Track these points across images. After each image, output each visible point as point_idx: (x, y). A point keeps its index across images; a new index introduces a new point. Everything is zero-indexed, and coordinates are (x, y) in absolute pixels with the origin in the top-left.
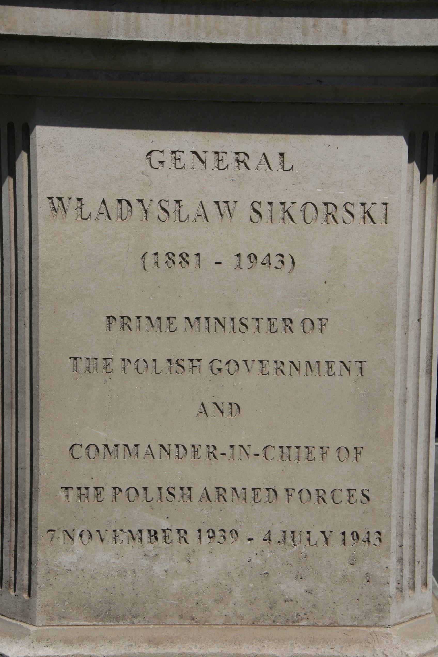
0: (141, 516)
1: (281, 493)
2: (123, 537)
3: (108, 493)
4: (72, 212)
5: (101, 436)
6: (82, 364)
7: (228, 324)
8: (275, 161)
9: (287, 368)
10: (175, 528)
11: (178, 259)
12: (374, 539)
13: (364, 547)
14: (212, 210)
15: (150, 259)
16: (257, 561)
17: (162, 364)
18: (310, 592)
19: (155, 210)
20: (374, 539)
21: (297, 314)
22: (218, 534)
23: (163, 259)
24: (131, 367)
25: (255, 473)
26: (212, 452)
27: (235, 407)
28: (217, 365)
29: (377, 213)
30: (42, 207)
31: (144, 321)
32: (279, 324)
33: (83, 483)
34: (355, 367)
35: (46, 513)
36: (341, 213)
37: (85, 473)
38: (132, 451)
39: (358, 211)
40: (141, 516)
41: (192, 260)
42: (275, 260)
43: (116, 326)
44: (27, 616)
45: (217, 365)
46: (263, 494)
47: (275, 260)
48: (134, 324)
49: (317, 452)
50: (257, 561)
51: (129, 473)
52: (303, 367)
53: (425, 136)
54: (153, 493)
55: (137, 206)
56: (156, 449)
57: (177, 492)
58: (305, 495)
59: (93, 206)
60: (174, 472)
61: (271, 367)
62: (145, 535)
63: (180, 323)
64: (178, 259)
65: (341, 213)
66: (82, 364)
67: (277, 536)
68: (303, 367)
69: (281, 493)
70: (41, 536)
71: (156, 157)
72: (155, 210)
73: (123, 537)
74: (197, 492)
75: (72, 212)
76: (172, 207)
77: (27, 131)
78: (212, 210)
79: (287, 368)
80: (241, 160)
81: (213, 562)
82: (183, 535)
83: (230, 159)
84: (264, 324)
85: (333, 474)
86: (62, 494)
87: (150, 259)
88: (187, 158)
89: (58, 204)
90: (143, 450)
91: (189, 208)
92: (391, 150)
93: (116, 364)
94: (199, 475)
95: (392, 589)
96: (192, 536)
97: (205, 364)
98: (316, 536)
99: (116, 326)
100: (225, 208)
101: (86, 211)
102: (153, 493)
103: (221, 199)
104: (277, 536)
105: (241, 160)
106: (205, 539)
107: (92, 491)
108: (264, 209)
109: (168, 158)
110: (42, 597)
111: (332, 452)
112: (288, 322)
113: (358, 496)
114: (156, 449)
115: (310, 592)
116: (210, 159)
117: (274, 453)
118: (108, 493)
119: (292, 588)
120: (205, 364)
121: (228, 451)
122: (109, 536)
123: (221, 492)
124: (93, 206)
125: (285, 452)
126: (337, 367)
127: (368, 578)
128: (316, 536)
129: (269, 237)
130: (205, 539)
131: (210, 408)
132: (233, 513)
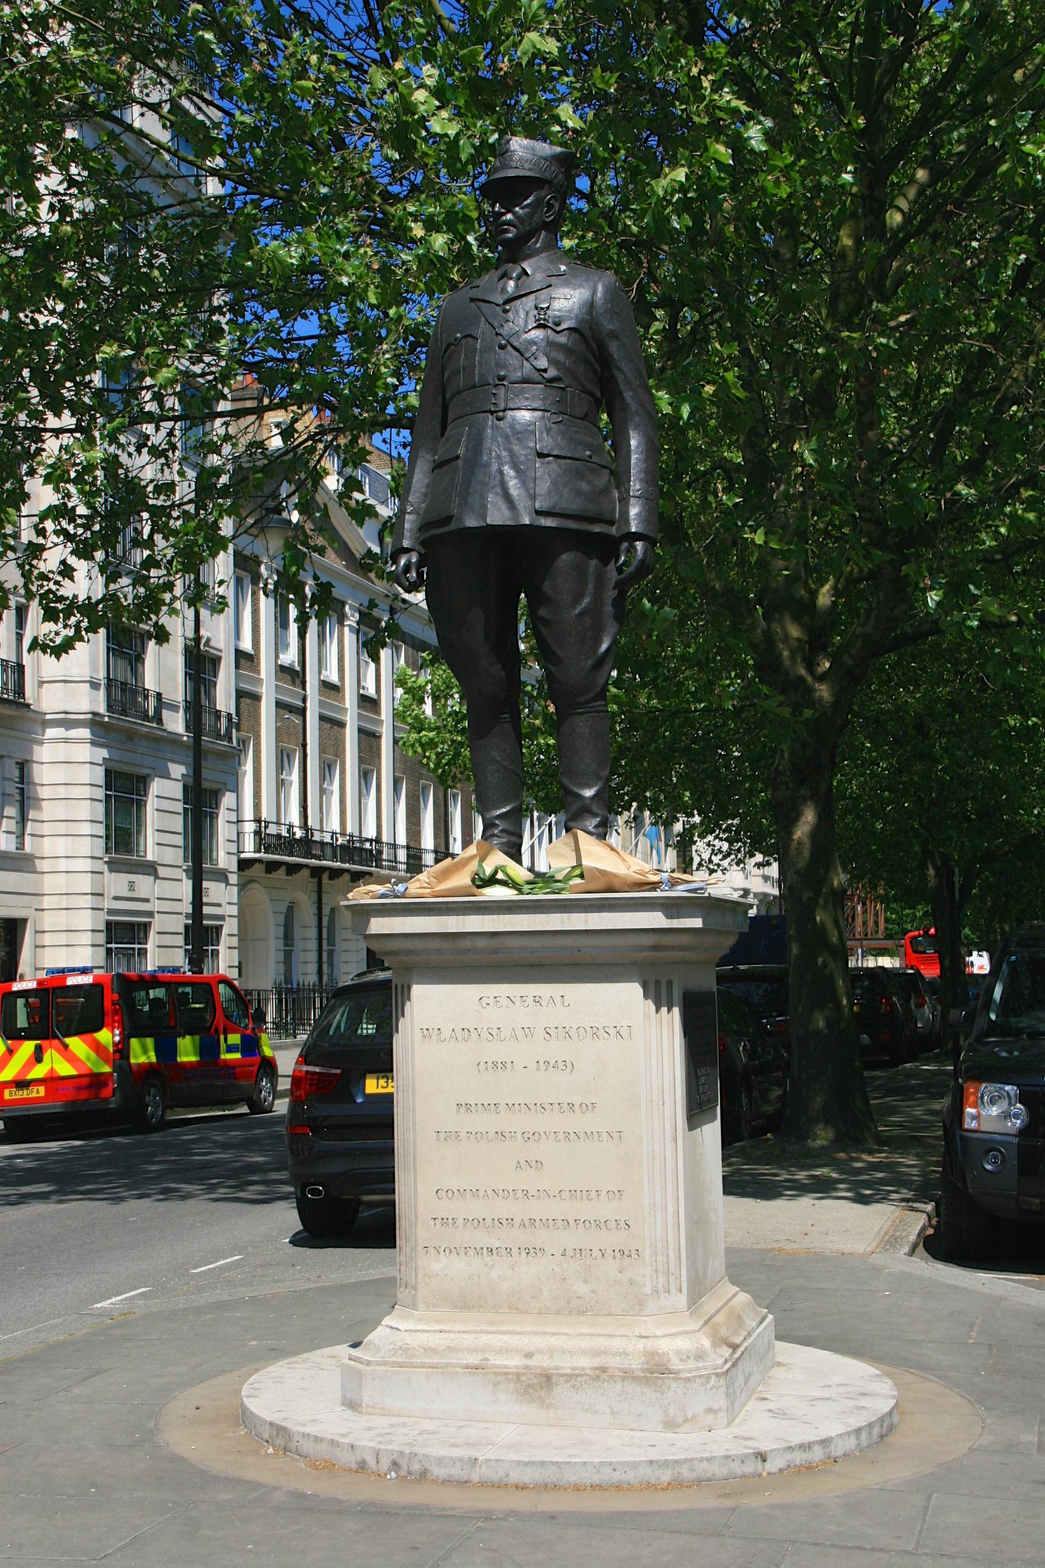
0: (482, 1238)
3: (460, 1222)
4: (434, 1037)
5: (454, 1184)
6: (442, 1136)
7: (533, 1107)
8: (558, 1000)
9: (572, 1137)
12: (634, 1255)
13: (628, 1260)
14: (520, 1033)
15: (482, 1065)
16: (557, 1270)
17: (492, 1135)
18: (593, 1291)
20: (634, 1255)
23: (490, 1065)
24: (473, 1137)
25: (554, 1209)
28: (527, 1135)
29: (625, 1032)
32: (565, 1107)
34: (616, 1136)
36: (602, 1033)
37: (445, 1208)
38: (475, 1193)
39: (612, 1031)
40: (482, 1238)
41: (509, 1065)
42: (561, 1065)
45: (527, 1135)
46: (560, 1223)
47: (561, 1065)
48: (473, 1108)
49: (593, 1194)
50: (557, 1270)
51: (474, 1209)
52: (582, 1135)
53: (658, 983)
54: (489, 1222)
56: (490, 1192)
57: (504, 1222)
59: (446, 1033)
60: (502, 1208)
61: (561, 1136)
63: (502, 1107)
65: (602, 1033)
66: (442, 1136)
67: (569, 1252)
68: (582, 1135)
69: (572, 1222)
73: (471, 1252)
74: (517, 1222)
77: (409, 988)
78: (520, 1033)
79: (572, 1137)
80: (537, 1000)
81: (530, 1271)
82: (509, 1251)
83: (530, 1001)
84: (556, 1107)
85: (606, 1210)
87: (482, 1065)
88: (504, 1001)
90: (481, 1193)
91: (506, 1032)
92: (630, 992)
93: (463, 1136)
94: (517, 1210)
95: (648, 1289)
96: (515, 1251)
97: (519, 1134)
98: (596, 1252)
100: (528, 1031)
101: (443, 1037)
105: (537, 1000)
108: (552, 1031)
109: (491, 1001)
110: (422, 1293)
111: (604, 1193)
112: (571, 1105)
113: (622, 1224)
114: (490, 1192)
115: (593, 1291)
116: (518, 1000)
118: (460, 1222)
119: (581, 1288)
120: (519, 1134)
121: (535, 1193)
123: (532, 1221)
124: (446, 1033)
126: (604, 1136)
128: (596, 1252)
129: (556, 1050)
130: (524, 1254)
131: (523, 1164)
132: (541, 1237)
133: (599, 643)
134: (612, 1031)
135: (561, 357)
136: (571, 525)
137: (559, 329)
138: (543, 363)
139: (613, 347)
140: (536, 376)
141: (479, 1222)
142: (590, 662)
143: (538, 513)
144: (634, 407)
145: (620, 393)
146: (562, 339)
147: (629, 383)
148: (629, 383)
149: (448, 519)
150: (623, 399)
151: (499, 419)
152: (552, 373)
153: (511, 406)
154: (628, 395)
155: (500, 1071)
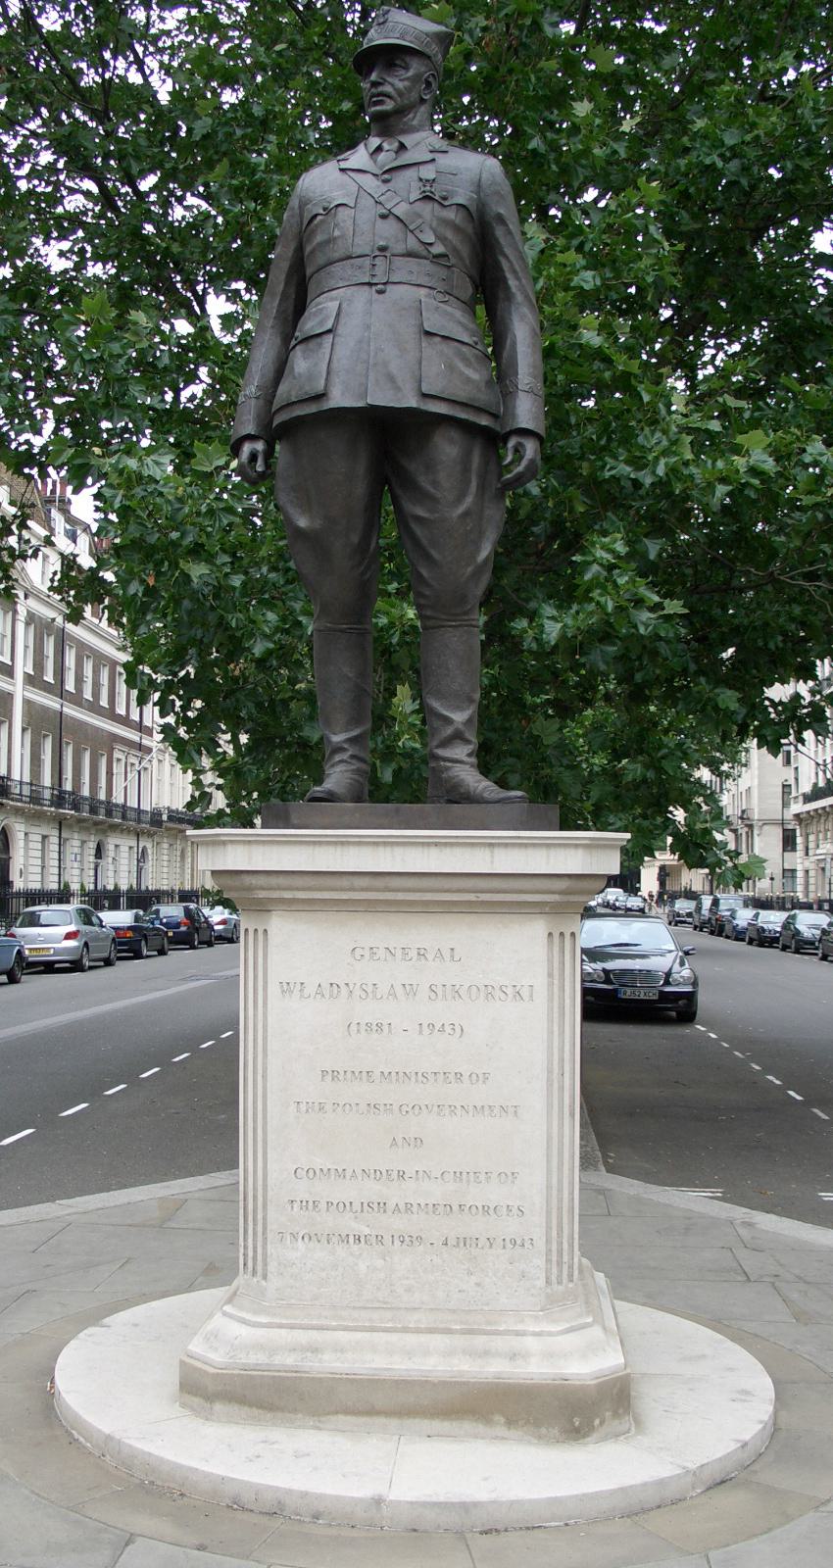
0: (350, 1224)
1: (455, 1208)
2: (335, 1239)
3: (323, 1206)
4: (296, 992)
5: (319, 1162)
6: (303, 1107)
8: (447, 954)
10: (374, 1233)
11: (374, 1027)
14: (399, 990)
15: (354, 1027)
17: (363, 1107)
19: (358, 992)
22: (407, 1239)
23: (363, 1027)
25: (436, 1192)
26: (401, 1175)
27: (419, 1141)
29: (525, 993)
30: (273, 989)
31: (349, 1074)
32: (452, 1077)
33: (306, 1197)
35: (275, 1218)
36: (498, 993)
37: (302, 1190)
38: (341, 1174)
39: (510, 991)
41: (386, 1028)
42: (448, 1029)
43: (329, 1078)
45: (404, 1108)
46: (441, 1209)
47: (448, 1029)
49: (482, 1177)
55: (344, 991)
56: (359, 1172)
58: (474, 1209)
59: (310, 989)
60: (372, 1190)
62: (351, 1239)
64: (374, 1027)
65: (498, 993)
66: (303, 1107)
67: (452, 1242)
69: (455, 1208)
71: (358, 952)
72: (358, 992)
73: (335, 1239)
74: (391, 1205)
75: (296, 992)
76: (370, 989)
78: (399, 990)
82: (380, 1239)
85: (494, 1193)
86: (289, 1207)
87: (354, 1027)
88: (381, 953)
89: (286, 988)
90: (349, 1173)
91: (383, 989)
94: (395, 1194)
96: (387, 1239)
97: (396, 1108)
98: (483, 1241)
99: (329, 1078)
100: (410, 990)
101: (306, 992)
102: (357, 1206)
103: (407, 982)
104: (452, 1242)
106: (397, 1242)
107: (311, 1204)
109: (367, 953)
111: (494, 1176)
112: (459, 1076)
113: (515, 1211)
114: (359, 1172)
117: (449, 1177)
118: (323, 1206)
120: (396, 1108)
122: (324, 1240)
123: (408, 1207)
124: (310, 989)
125: (458, 1175)
130: (397, 1242)
131: (400, 1141)
133: (478, 550)
134: (510, 991)
135: (449, 234)
136: (462, 415)
137: (446, 203)
138: (430, 238)
139: (499, 232)
140: (420, 249)
141: (345, 1206)
142: (470, 569)
143: (425, 396)
144: (519, 297)
145: (505, 280)
146: (451, 214)
147: (514, 272)
148: (514, 272)
149: (320, 397)
150: (507, 288)
151: (380, 292)
153: (394, 279)
154: (512, 283)
155: (375, 1036)
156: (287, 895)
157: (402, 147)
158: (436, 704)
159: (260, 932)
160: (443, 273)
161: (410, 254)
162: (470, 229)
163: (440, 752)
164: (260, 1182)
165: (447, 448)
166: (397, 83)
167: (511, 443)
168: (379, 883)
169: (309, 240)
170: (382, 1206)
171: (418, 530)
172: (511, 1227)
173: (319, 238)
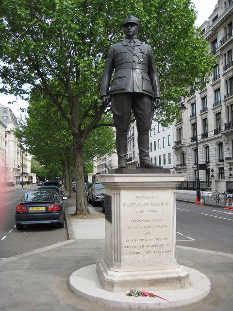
0: (137, 250)
21: (158, 219)
25: (153, 243)
26: (146, 240)
27: (150, 233)
30: (122, 205)
35: (123, 250)
37: (128, 244)
38: (135, 240)
44: (119, 266)
51: (135, 244)
59: (129, 205)
60: (140, 243)
70: (122, 254)
85: (164, 242)
88: (142, 197)
89: (124, 205)
94: (145, 243)
100: (147, 204)
110: (123, 263)
124: (129, 205)
125: (157, 239)
127: (169, 257)
129: (154, 208)
138: (142, 60)
139: (152, 60)
140: (140, 62)
149: (124, 89)
152: (143, 62)
156: (125, 186)
157: (134, 42)
158: (141, 148)
159: (115, 194)
160: (144, 67)
161: (139, 63)
162: (148, 58)
163: (143, 158)
164: (119, 243)
165: (146, 100)
166: (133, 29)
167: (157, 100)
168: (143, 184)
169: (117, 58)
170: (143, 246)
171: (140, 116)
172: (165, 249)
173: (120, 58)
